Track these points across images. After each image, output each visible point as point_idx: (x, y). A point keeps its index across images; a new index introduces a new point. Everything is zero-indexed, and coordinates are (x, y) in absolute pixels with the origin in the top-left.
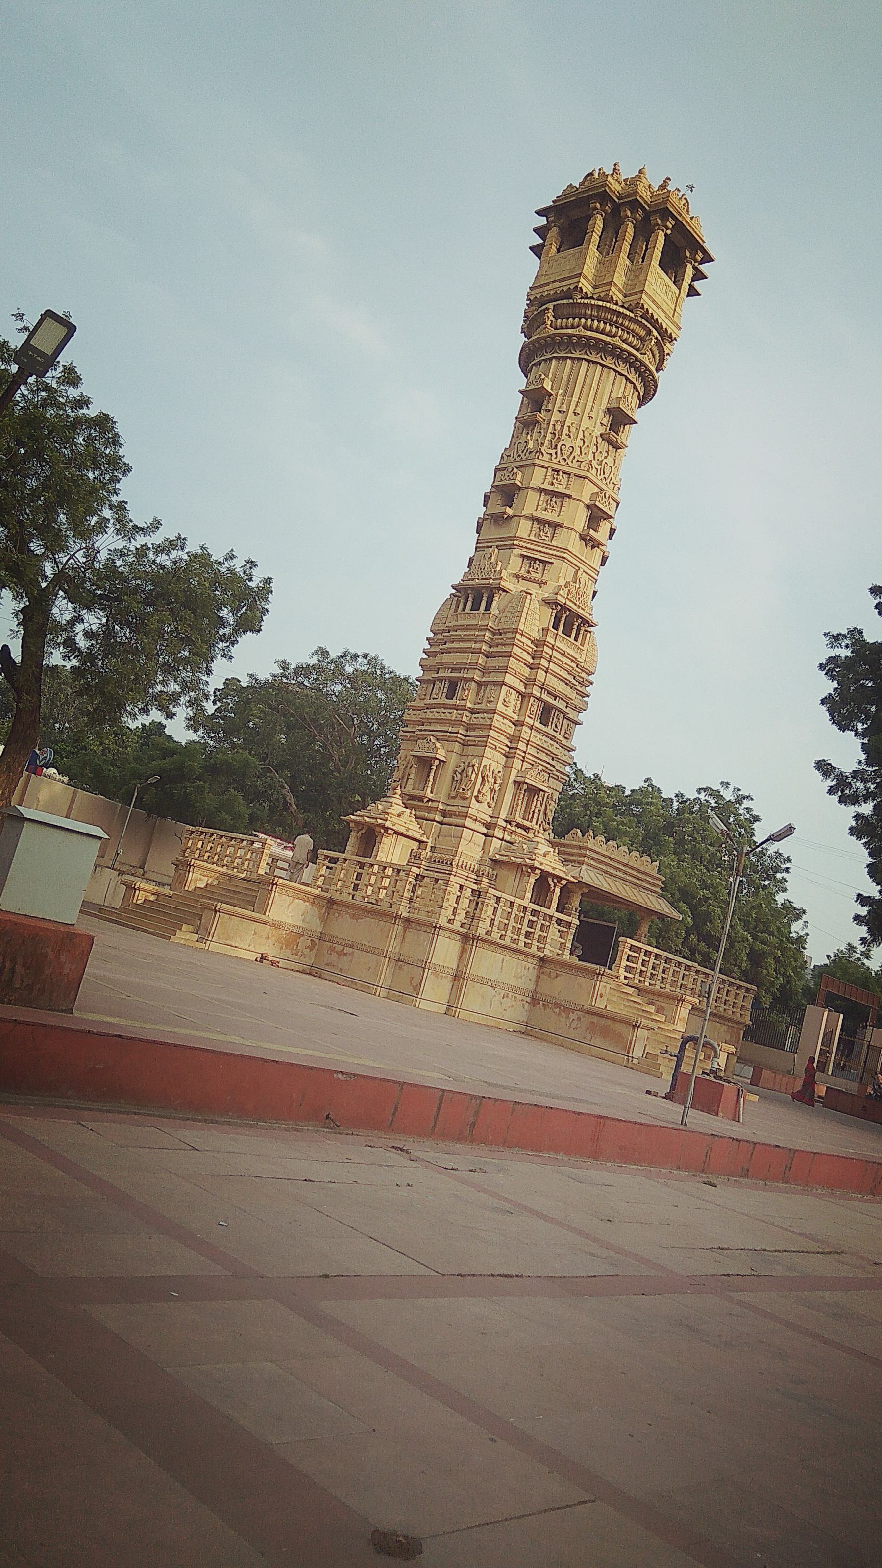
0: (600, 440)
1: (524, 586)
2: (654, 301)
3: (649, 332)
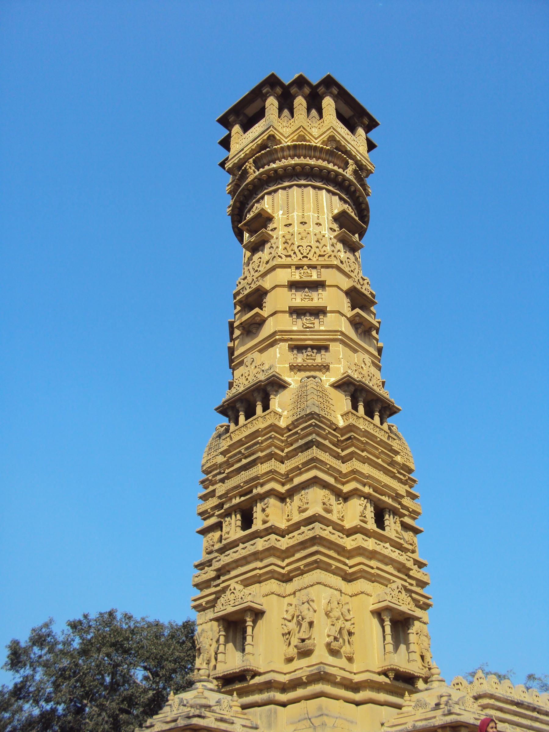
0: (335, 241)
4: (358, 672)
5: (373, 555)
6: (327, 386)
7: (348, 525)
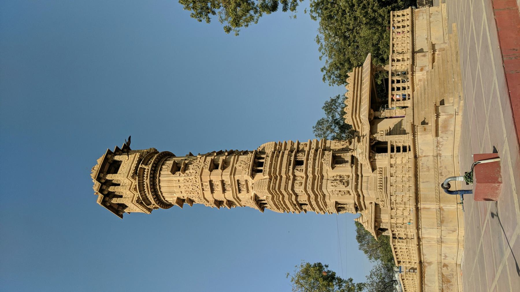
1: (250, 189)
2: (129, 171)
3: (141, 168)
4: (352, 175)
5: (314, 169)
6: (253, 181)
7: (305, 177)
